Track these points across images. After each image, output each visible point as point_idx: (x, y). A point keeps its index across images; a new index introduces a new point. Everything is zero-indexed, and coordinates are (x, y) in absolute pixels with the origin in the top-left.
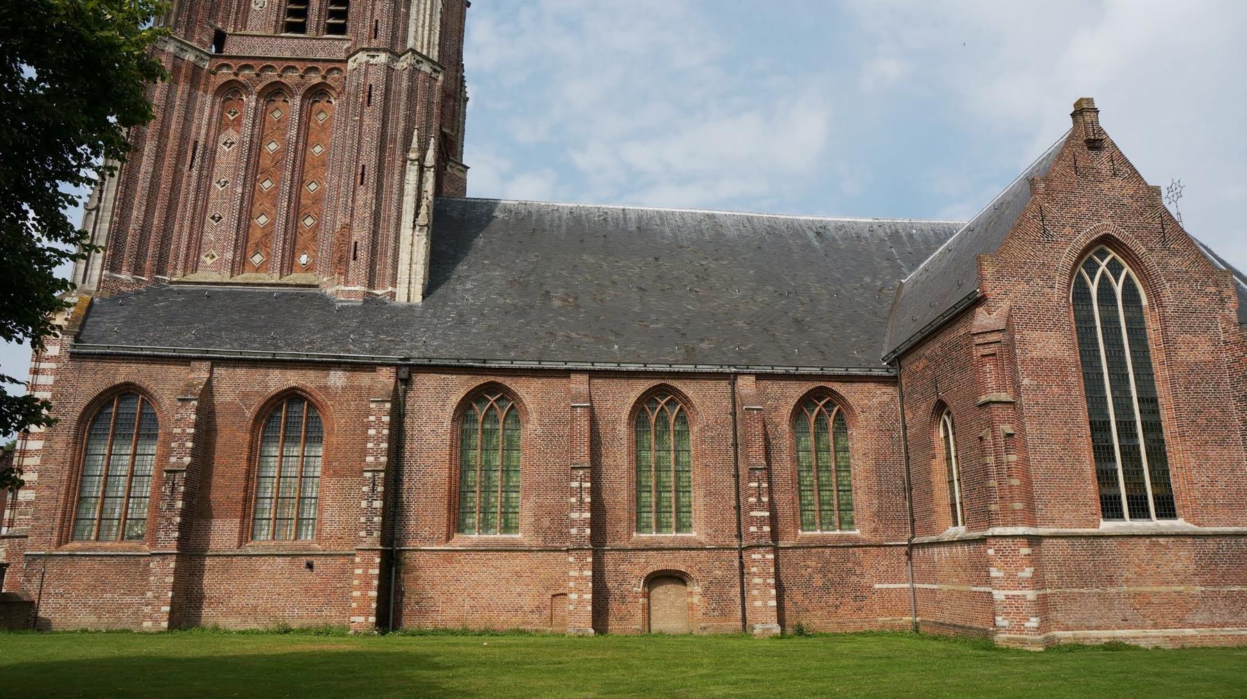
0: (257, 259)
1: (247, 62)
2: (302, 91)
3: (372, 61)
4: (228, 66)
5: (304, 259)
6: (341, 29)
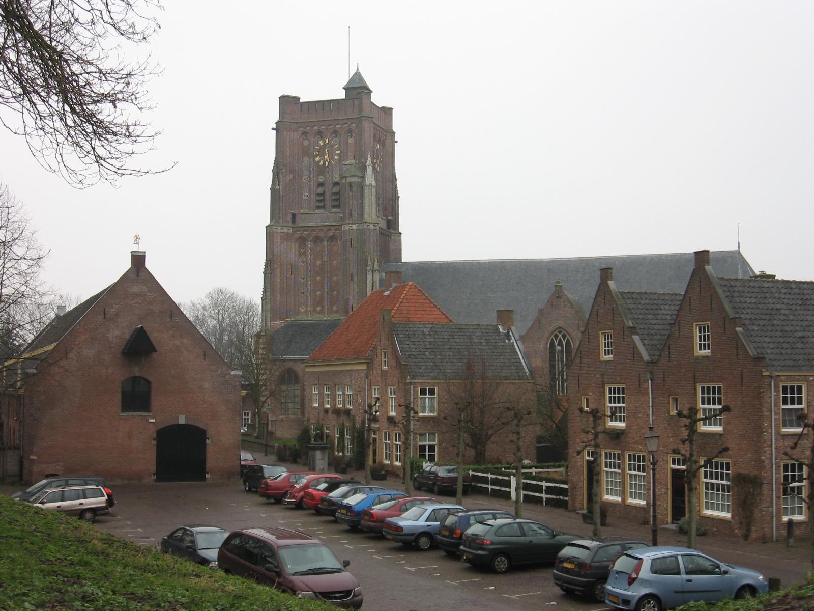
0: (319, 309)
1: (305, 228)
2: (326, 239)
3: (351, 228)
4: (298, 231)
5: (335, 308)
6: (338, 206)
